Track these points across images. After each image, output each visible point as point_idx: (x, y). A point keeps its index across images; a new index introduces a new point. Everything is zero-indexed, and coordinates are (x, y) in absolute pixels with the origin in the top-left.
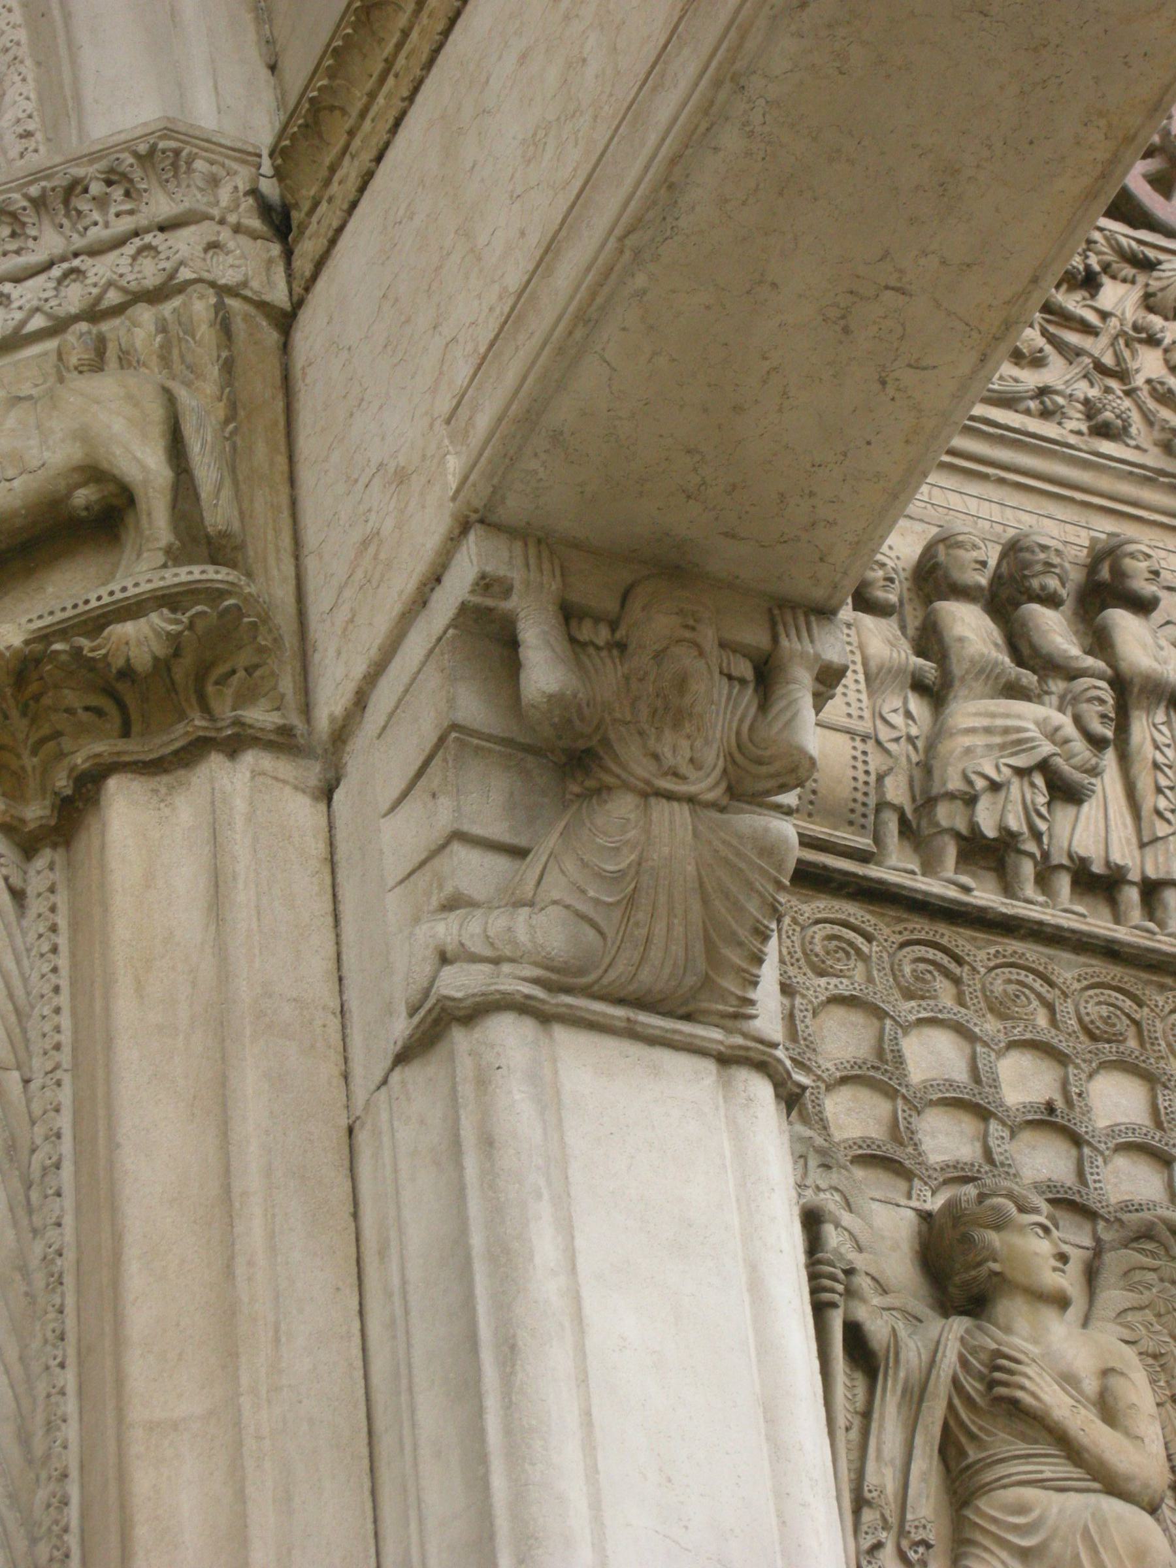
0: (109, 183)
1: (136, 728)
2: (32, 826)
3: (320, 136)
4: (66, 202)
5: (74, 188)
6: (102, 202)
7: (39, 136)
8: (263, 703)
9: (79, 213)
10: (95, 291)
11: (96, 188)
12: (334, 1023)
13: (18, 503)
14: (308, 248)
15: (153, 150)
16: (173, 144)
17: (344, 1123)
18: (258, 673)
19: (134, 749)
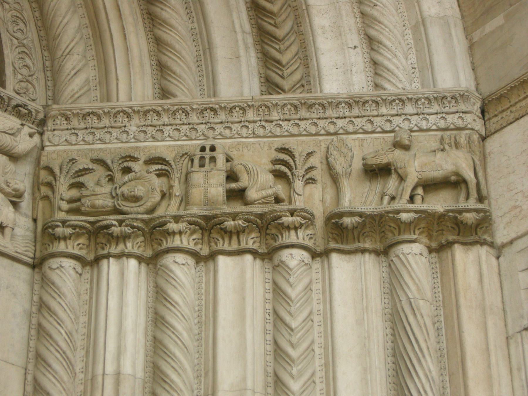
0: (452, 98)
1: (461, 234)
2: (433, 248)
3: (500, 101)
4: (442, 100)
5: (444, 97)
6: (450, 102)
7: (417, 69)
8: (487, 234)
9: (444, 103)
10: (449, 124)
11: (449, 99)
12: (502, 312)
13: (440, 176)
14: (493, 125)
15: (464, 94)
16: (468, 94)
17: (506, 336)
18: (488, 228)
19: (461, 239)
